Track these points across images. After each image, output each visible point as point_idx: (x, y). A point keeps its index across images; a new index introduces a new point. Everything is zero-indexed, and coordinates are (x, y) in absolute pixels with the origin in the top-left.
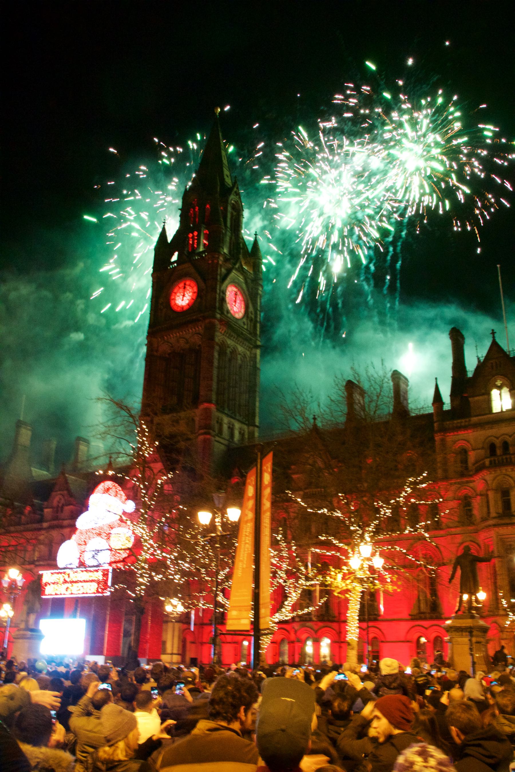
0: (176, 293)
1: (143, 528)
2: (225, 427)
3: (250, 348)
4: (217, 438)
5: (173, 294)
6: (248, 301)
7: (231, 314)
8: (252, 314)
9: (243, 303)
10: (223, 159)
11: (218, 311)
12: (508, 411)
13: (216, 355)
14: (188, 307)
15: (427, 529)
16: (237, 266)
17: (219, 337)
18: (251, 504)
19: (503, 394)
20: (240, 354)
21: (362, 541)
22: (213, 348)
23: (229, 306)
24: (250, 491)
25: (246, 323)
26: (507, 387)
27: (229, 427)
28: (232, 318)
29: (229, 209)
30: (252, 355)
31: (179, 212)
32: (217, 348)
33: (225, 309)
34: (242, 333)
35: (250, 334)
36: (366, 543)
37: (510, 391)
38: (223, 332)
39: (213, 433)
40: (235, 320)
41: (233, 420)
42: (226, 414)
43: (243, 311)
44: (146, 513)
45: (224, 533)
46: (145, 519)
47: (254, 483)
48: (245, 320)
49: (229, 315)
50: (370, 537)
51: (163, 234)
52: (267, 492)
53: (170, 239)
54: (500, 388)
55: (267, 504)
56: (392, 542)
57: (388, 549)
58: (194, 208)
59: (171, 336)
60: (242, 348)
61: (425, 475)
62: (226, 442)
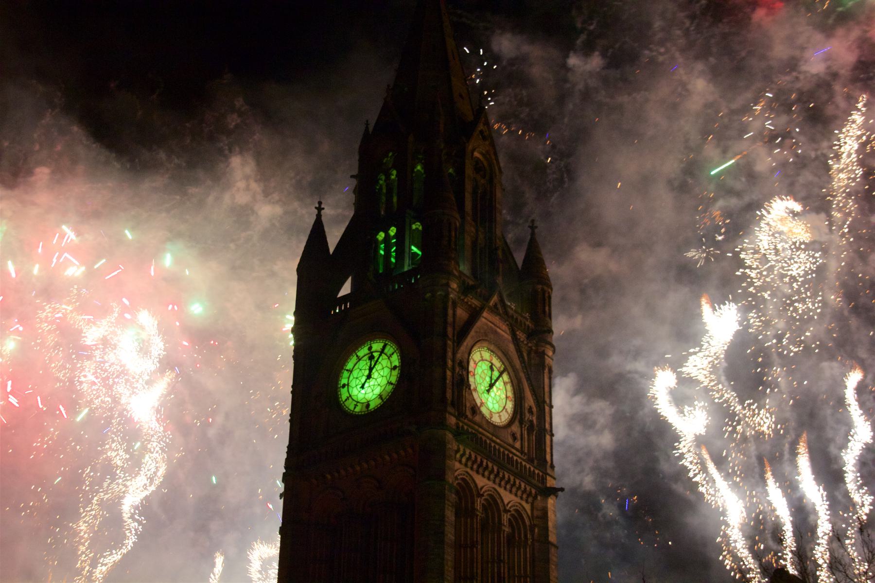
0: (351, 371)
3: (530, 495)
5: (345, 374)
6: (519, 382)
7: (483, 416)
9: (509, 387)
11: (450, 409)
13: (450, 514)
14: (379, 401)
16: (492, 303)
17: (457, 469)
20: (506, 511)
23: (474, 394)
28: (485, 426)
29: (469, 171)
30: (536, 513)
31: (354, 182)
33: (468, 405)
34: (510, 460)
35: (530, 461)
38: (464, 460)
40: (491, 430)
43: (510, 406)
48: (515, 428)
49: (477, 418)
51: (317, 233)
58: (388, 176)
59: (343, 472)
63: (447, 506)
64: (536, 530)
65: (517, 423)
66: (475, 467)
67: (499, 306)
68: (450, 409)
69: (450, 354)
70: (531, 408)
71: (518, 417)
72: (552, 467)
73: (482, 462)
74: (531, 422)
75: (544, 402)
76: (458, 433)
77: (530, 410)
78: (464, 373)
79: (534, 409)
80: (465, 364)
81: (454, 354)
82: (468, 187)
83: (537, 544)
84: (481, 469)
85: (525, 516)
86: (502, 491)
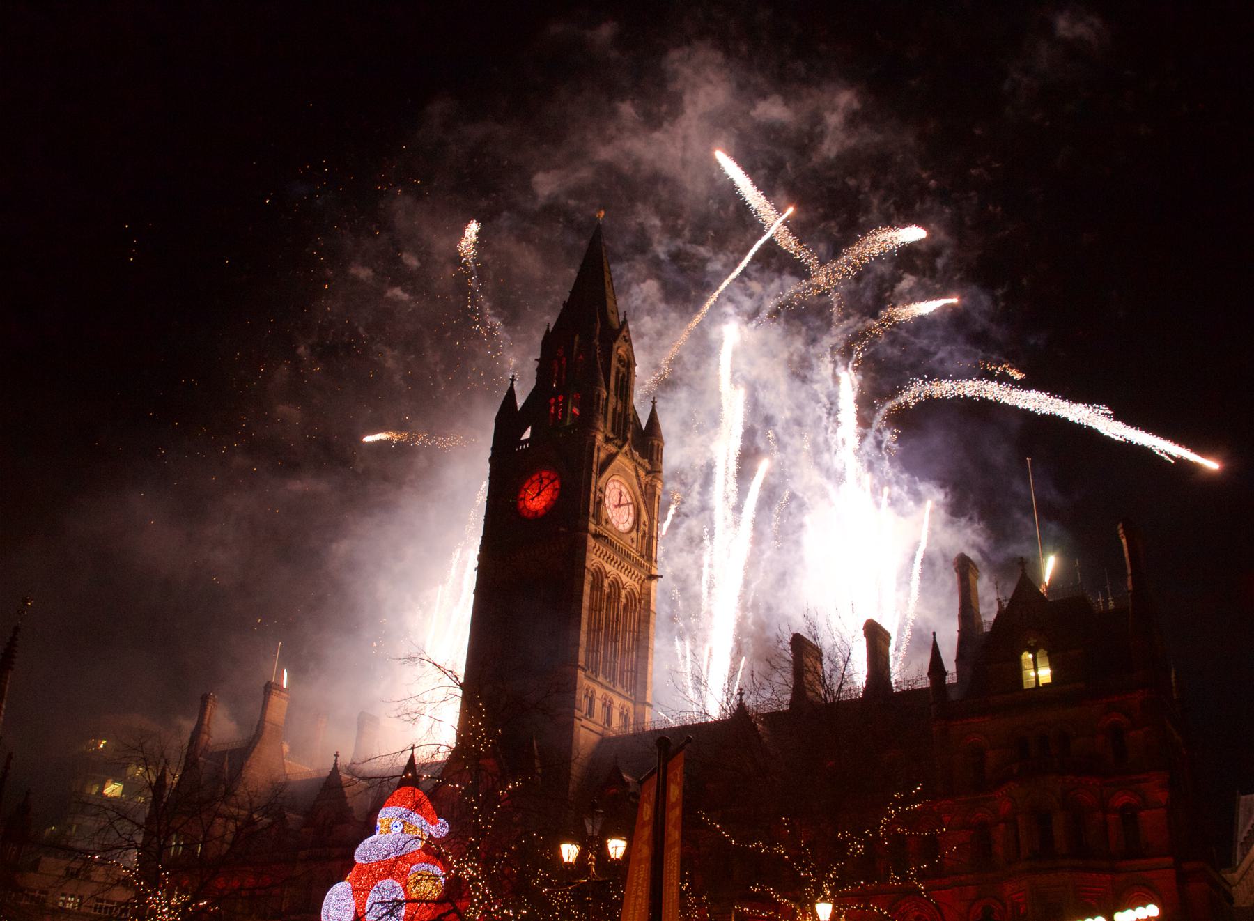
1: (473, 867)
2: (598, 704)
4: (584, 722)
6: (638, 505)
8: (644, 524)
10: (607, 286)
12: (1045, 685)
15: (922, 876)
18: (646, 832)
19: (1038, 660)
21: (817, 896)
22: (583, 577)
23: (609, 511)
24: (647, 812)
25: (635, 540)
26: (1045, 649)
27: (604, 705)
29: (614, 362)
30: (643, 591)
32: (588, 578)
33: (603, 517)
34: (629, 556)
35: (642, 556)
36: (824, 900)
37: (1049, 655)
38: (598, 553)
39: (577, 713)
41: (610, 694)
42: (617, 693)
43: (631, 520)
44: (478, 843)
45: (601, 879)
46: (477, 853)
47: (652, 799)
48: (634, 534)
49: (609, 527)
50: (830, 888)
52: (675, 814)
53: (520, 403)
54: (1033, 651)
55: (674, 835)
56: (864, 897)
57: (858, 908)
60: (628, 579)
61: (918, 788)
62: (599, 729)
63: (585, 584)
64: (643, 602)
65: (635, 531)
66: (606, 558)
67: (628, 454)
68: (591, 519)
69: (593, 483)
70: (644, 522)
71: (636, 527)
72: (656, 561)
73: (610, 555)
74: (644, 531)
75: (653, 518)
76: (597, 536)
77: (644, 524)
78: (603, 496)
79: (647, 523)
80: (603, 490)
81: (596, 482)
82: (613, 373)
83: (642, 611)
84: (610, 560)
85: (636, 593)
86: (622, 575)
